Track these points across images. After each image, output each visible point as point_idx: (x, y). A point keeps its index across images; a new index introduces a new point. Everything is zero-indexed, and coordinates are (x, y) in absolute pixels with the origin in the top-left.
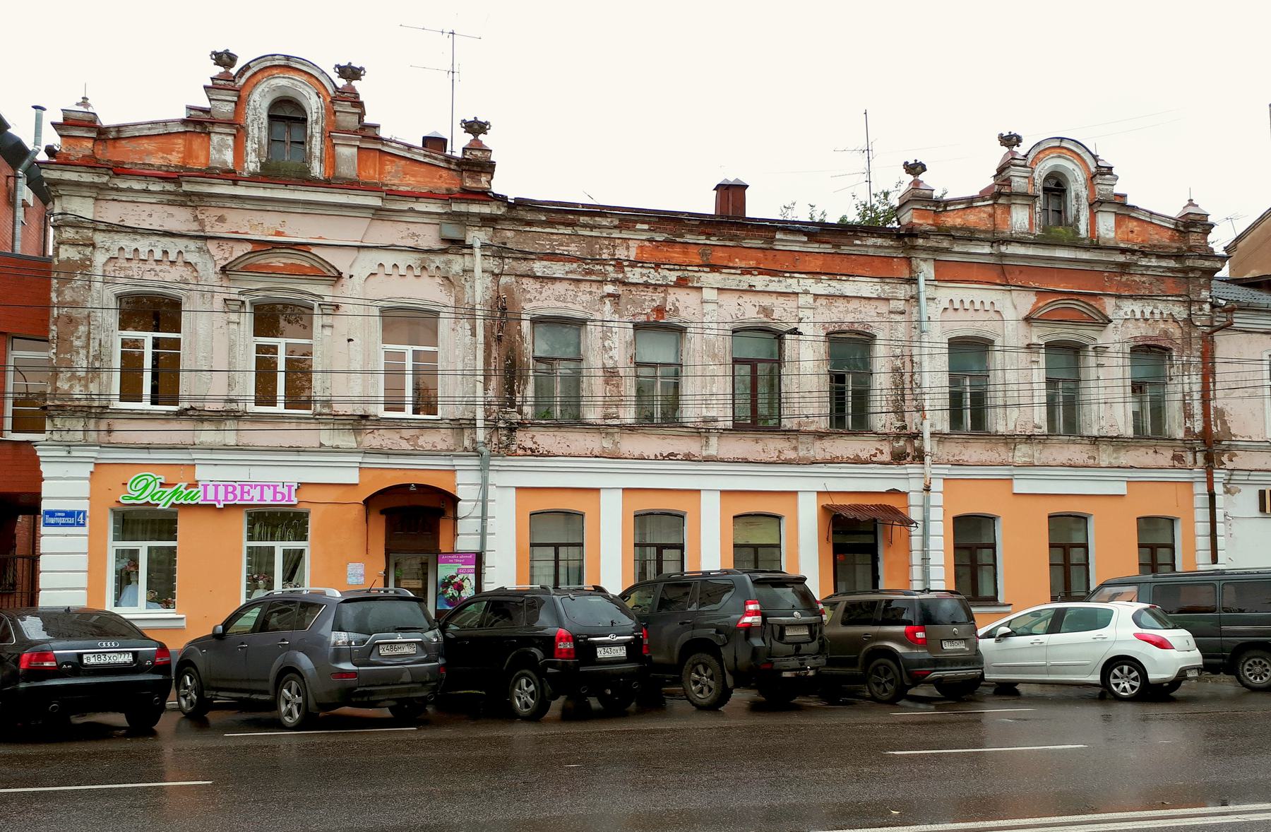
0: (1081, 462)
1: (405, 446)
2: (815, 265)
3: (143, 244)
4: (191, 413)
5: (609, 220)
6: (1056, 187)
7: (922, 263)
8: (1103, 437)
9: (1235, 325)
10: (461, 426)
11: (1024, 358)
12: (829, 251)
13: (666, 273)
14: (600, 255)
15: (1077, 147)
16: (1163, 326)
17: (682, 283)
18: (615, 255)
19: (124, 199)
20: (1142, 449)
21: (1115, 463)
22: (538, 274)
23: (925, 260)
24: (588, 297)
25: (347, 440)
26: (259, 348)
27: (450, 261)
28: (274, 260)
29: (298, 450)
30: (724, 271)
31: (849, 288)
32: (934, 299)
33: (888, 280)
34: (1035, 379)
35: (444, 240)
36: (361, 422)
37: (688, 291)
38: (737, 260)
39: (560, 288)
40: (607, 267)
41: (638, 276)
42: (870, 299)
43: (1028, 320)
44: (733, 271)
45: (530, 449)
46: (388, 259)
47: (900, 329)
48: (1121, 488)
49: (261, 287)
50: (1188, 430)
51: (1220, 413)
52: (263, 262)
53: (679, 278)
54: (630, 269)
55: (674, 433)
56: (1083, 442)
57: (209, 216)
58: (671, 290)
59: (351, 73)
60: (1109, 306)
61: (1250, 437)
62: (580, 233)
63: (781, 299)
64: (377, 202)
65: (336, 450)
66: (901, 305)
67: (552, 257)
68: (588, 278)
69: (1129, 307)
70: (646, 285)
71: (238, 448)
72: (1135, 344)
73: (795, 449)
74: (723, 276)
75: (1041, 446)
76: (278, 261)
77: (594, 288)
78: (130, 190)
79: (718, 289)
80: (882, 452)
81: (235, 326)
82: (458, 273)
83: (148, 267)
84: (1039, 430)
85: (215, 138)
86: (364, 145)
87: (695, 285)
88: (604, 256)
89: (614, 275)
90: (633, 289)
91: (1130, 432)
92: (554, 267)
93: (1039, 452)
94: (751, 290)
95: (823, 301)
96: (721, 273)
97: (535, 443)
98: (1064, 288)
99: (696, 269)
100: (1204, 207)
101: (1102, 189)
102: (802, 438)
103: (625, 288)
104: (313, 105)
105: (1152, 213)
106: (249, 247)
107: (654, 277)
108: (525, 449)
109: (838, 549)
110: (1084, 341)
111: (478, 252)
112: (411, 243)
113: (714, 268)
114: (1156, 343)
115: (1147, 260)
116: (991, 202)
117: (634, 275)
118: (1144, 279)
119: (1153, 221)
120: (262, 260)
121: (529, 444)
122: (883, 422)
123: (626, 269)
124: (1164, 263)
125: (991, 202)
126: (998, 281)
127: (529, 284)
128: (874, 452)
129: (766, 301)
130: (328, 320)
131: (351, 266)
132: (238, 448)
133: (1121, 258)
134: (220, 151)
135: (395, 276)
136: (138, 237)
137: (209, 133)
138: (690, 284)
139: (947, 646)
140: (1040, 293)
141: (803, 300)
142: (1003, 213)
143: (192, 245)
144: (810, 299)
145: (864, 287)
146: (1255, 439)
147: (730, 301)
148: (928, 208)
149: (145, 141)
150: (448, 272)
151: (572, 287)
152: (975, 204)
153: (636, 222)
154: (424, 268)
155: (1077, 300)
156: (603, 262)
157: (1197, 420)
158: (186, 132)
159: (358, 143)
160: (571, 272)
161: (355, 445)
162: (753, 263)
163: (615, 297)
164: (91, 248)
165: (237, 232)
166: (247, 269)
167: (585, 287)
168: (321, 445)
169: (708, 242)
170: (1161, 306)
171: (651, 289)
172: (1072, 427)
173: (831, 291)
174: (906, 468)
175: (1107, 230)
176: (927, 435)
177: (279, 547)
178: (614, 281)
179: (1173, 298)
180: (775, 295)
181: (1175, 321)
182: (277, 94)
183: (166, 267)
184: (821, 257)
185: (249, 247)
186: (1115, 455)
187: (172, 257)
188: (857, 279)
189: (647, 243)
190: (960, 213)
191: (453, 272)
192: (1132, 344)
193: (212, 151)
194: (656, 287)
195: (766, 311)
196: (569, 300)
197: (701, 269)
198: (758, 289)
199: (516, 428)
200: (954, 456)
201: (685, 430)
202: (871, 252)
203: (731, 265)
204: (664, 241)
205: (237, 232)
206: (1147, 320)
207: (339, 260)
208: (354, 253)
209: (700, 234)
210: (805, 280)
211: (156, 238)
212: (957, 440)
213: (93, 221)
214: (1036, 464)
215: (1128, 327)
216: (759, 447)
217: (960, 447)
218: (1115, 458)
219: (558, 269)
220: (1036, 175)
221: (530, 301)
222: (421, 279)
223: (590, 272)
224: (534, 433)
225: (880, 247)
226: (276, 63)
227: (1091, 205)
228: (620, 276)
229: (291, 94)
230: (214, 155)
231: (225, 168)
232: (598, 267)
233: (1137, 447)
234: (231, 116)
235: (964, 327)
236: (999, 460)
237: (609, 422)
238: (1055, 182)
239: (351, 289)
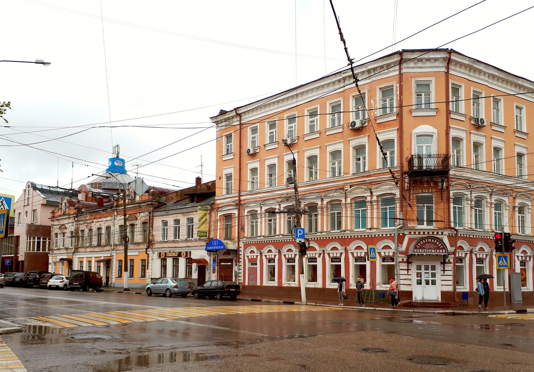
21: (137, 248)
48: (137, 253)
51: (153, 236)
53: (92, 221)
69: (142, 214)
113: (95, 219)
139: (44, 281)
147: (97, 224)
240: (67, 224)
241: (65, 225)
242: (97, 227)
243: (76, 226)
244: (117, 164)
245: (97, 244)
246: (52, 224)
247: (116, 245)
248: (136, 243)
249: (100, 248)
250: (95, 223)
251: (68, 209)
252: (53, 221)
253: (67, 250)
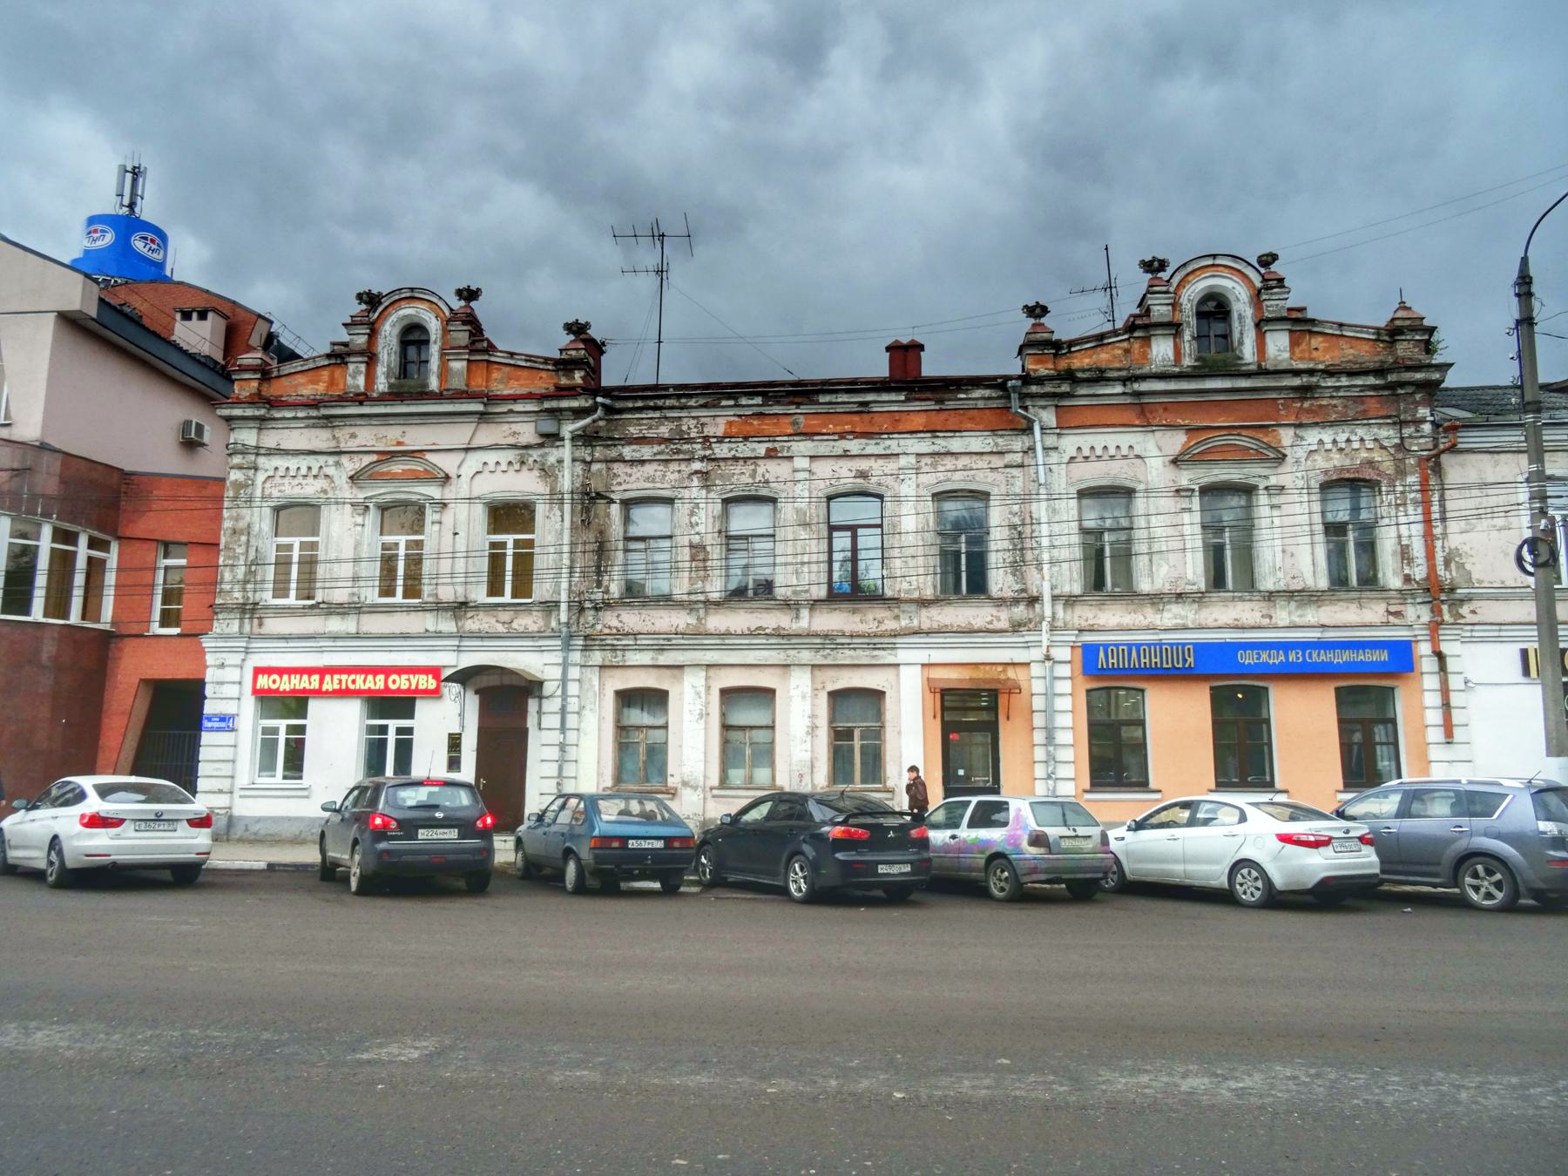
0: (1252, 623)
1: (501, 629)
2: (919, 421)
3: (292, 463)
4: (321, 606)
5: (694, 400)
6: (1215, 309)
7: (1041, 410)
8: (1279, 592)
9: (1459, 446)
10: (550, 607)
11: (1169, 504)
12: (932, 408)
13: (755, 445)
14: (689, 434)
15: (1237, 263)
16: (1366, 455)
17: (771, 455)
18: (702, 432)
19: (280, 426)
20: (1341, 603)
21: (1298, 620)
22: (627, 458)
23: (1044, 407)
24: (676, 475)
25: (448, 625)
26: (385, 547)
27: (546, 454)
28: (393, 467)
29: (405, 636)
30: (816, 438)
31: (956, 444)
32: (1056, 448)
33: (1000, 433)
34: (1187, 530)
35: (543, 435)
36: (461, 608)
37: (779, 461)
38: (831, 426)
39: (649, 469)
40: (694, 446)
41: (726, 451)
42: (982, 454)
43: (1175, 462)
44: (825, 437)
45: (616, 628)
46: (491, 457)
47: (1018, 483)
49: (383, 492)
50: (1407, 579)
52: (385, 470)
53: (768, 450)
54: (718, 445)
55: (762, 606)
56: (1254, 598)
57: (343, 434)
58: (760, 462)
59: (469, 295)
60: (1286, 436)
61: (1503, 583)
62: (668, 415)
63: (881, 462)
64: (480, 408)
65: (439, 635)
66: (1018, 458)
67: (642, 440)
68: (675, 457)
69: (1312, 436)
70: (735, 459)
71: (357, 636)
72: (1327, 478)
73: (897, 618)
74: (816, 443)
75: (1196, 606)
76: (397, 468)
77: (683, 466)
78: (284, 419)
79: (811, 457)
80: (999, 620)
81: (359, 528)
82: (553, 465)
83: (296, 481)
84: (1191, 587)
85: (351, 367)
86: (473, 358)
87: (785, 454)
88: (692, 435)
89: (702, 453)
90: (722, 464)
91: (1323, 583)
92: (643, 450)
93: (1193, 612)
94: (846, 455)
95: (928, 460)
96: (813, 440)
97: (621, 622)
98: (1224, 422)
99: (786, 438)
100: (1419, 309)
101: (1273, 306)
102: (905, 607)
103: (713, 464)
104: (434, 326)
105: (1341, 325)
106: (374, 458)
107: (744, 449)
108: (610, 627)
109: (947, 729)
110: (1252, 481)
111: (567, 443)
112: (511, 441)
113: (808, 435)
114: (1356, 475)
115: (1334, 379)
116: (1126, 337)
117: (721, 450)
118: (1334, 402)
119: (1345, 333)
120: (384, 468)
121: (614, 623)
122: (1000, 586)
123: (714, 445)
124: (1359, 381)
125: (1126, 337)
126: (1137, 422)
127: (619, 468)
128: (989, 618)
129: (864, 465)
130: (436, 517)
131: (459, 467)
132: (357, 636)
133: (1297, 382)
134: (354, 378)
135: (498, 473)
136: (290, 457)
137: (346, 363)
138: (780, 455)
140: (1190, 430)
141: (903, 461)
142: (1141, 347)
143: (331, 460)
144: (912, 459)
145: (976, 442)
146: (1508, 584)
147: (824, 469)
148: (1046, 351)
149: (299, 376)
150: (543, 464)
151: (661, 468)
152: (1106, 341)
153: (720, 399)
154: (523, 463)
155: (1239, 435)
156: (690, 441)
157: (1418, 565)
158: (329, 365)
159: (467, 357)
160: (659, 453)
161: (455, 630)
162: (848, 428)
163: (704, 475)
164: (253, 471)
165: (365, 446)
166: (371, 478)
167: (674, 466)
168: (427, 631)
169: (799, 411)
170: (1361, 432)
171: (741, 462)
172: (1248, 583)
173: (936, 448)
174: (1023, 636)
175: (1279, 350)
176: (1047, 598)
177: (393, 724)
178: (702, 459)
179: (1378, 421)
180: (873, 459)
181: (1383, 448)
182: (405, 322)
183: (310, 480)
184: (924, 415)
185: (374, 458)
186: (1299, 612)
187: (315, 471)
188: (964, 434)
189: (736, 419)
190: (1089, 352)
191: (549, 463)
192: (1322, 478)
193: (349, 378)
194: (746, 459)
195: (863, 475)
196: (657, 480)
197: (791, 438)
198: (853, 453)
199: (601, 608)
200: (1087, 620)
201: (773, 602)
202: (981, 404)
203: (824, 431)
204: (753, 415)
205: (365, 446)
206: (1341, 450)
207: (447, 463)
208: (461, 455)
209: (792, 403)
210: (907, 441)
211: (303, 457)
212: (1090, 603)
213: (257, 447)
214: (1191, 626)
215: (1315, 460)
216: (857, 618)
217: (1094, 610)
218: (1300, 616)
219: (646, 452)
220: (1184, 300)
221: (620, 484)
222: (521, 473)
223: (679, 452)
224: (620, 612)
225: (989, 398)
226: (403, 296)
227: (1258, 325)
228: (708, 453)
229: (416, 320)
230: (350, 381)
231: (358, 391)
232: (686, 447)
233: (1332, 602)
234: (365, 347)
235: (1095, 474)
236: (1145, 623)
237: (693, 597)
238: (1214, 304)
239: (461, 488)
240: (460, 456)
241: (429, 456)
242: (822, 488)
243: (579, 468)
244: (145, 250)
246: (254, 444)
247: (1070, 601)
248: (1290, 595)
251: (458, 366)
252: (260, 429)
253: (456, 618)
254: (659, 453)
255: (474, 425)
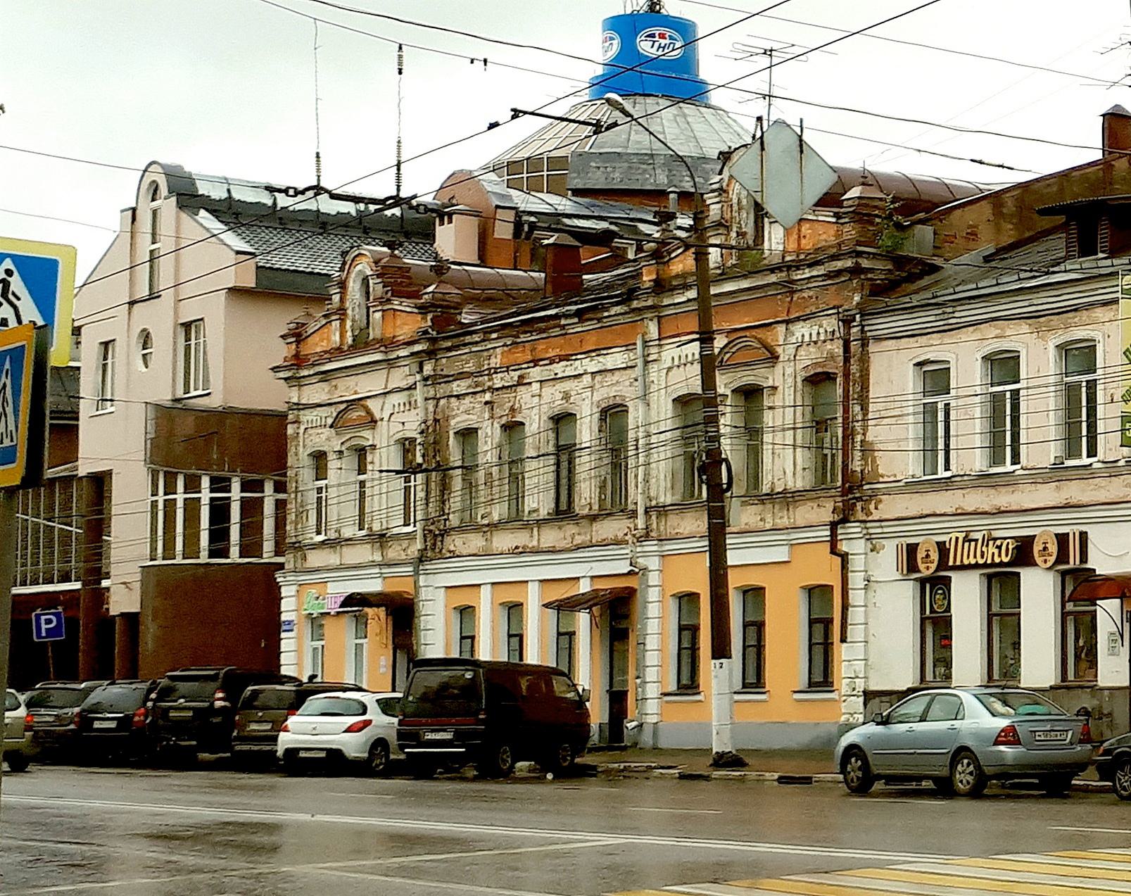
30: (541, 363)
53: (521, 377)
113: (535, 362)
129: (567, 385)
139: (254, 727)
147: (548, 391)
154: (410, 403)
185: (343, 406)
240: (379, 401)
241: (369, 403)
242: (547, 411)
243: (431, 404)
245: (553, 505)
249: (571, 529)
250: (536, 386)
254: (469, 387)
255: (385, 371)
